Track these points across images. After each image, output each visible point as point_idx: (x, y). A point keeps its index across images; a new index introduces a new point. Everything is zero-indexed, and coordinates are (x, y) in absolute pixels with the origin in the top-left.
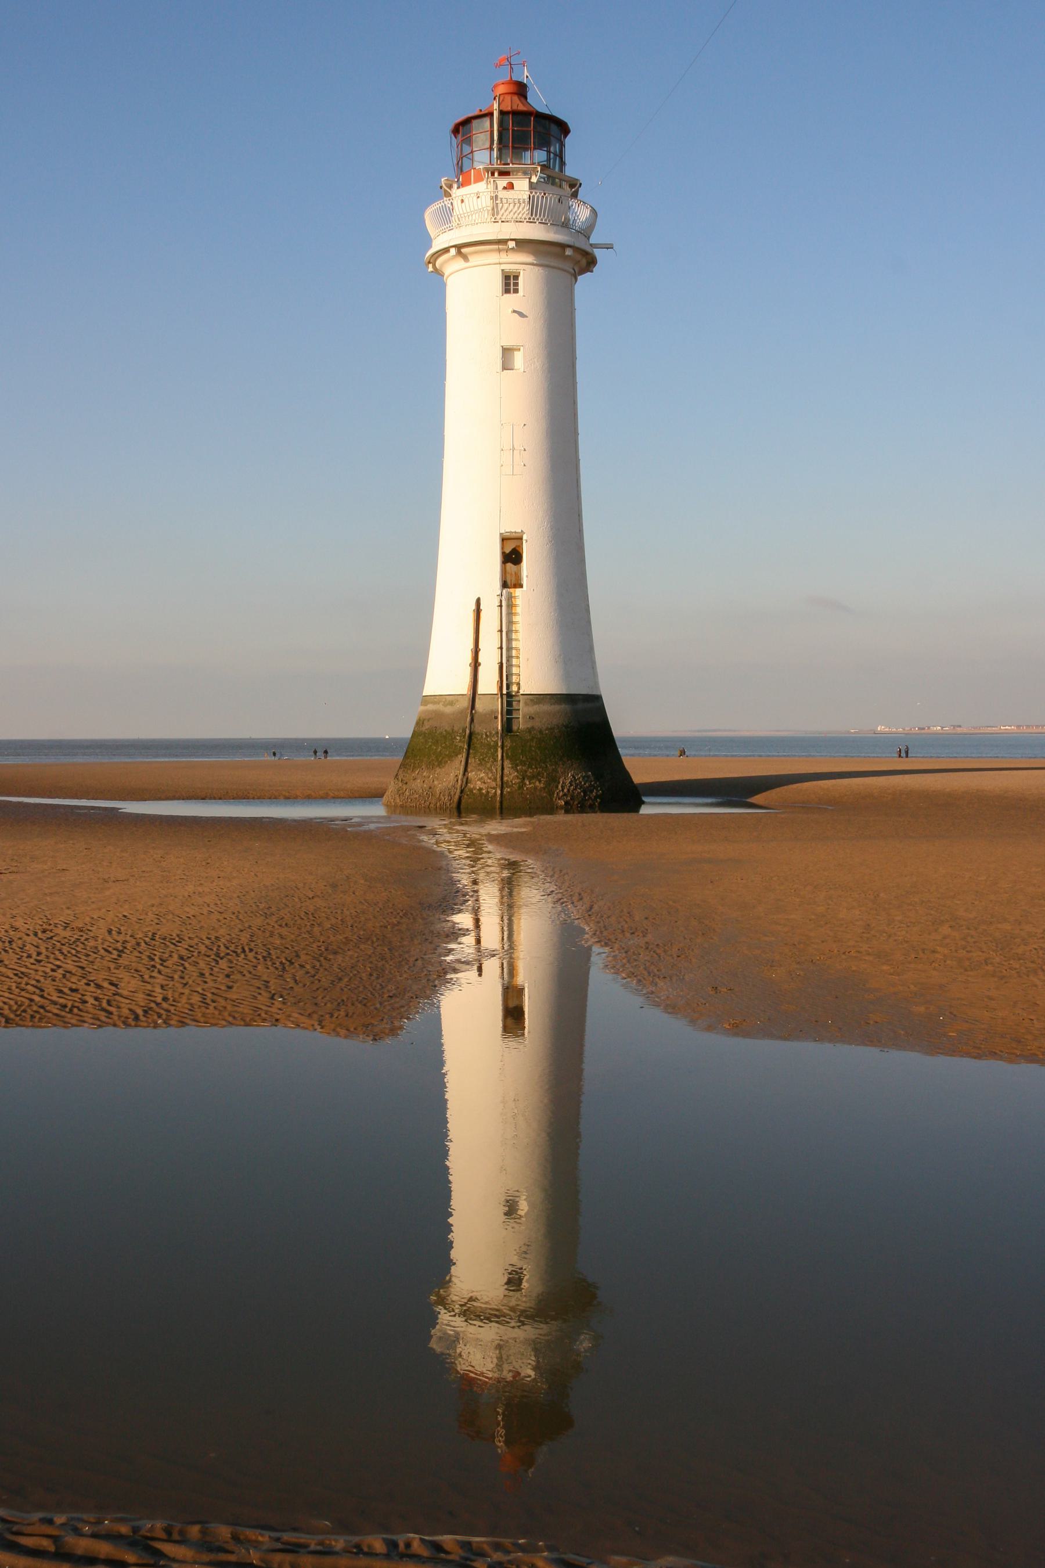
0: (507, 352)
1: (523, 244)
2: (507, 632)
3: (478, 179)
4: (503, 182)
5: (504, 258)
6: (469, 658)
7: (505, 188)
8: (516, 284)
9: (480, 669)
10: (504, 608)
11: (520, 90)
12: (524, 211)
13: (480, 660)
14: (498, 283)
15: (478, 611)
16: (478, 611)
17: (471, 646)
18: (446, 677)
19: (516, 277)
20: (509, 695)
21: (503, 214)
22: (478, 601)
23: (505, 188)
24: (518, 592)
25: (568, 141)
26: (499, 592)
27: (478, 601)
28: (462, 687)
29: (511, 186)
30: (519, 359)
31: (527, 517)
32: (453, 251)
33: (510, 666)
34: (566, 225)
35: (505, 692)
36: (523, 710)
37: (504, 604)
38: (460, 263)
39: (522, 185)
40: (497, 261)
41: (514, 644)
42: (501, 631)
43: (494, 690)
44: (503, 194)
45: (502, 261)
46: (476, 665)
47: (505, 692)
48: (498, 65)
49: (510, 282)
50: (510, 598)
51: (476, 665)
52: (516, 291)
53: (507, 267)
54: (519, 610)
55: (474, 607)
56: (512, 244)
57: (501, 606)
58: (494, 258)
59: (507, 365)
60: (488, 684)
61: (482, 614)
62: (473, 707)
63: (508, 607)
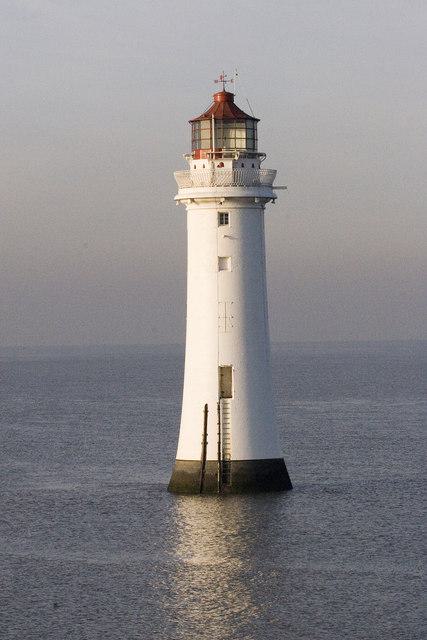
0: (221, 260)
1: (227, 199)
3: (203, 158)
4: (217, 163)
6: (202, 438)
8: (227, 219)
11: (228, 98)
12: (230, 179)
14: (215, 221)
15: (206, 412)
16: (206, 412)
18: (189, 449)
19: (227, 215)
20: (224, 461)
21: (218, 182)
24: (229, 400)
25: (259, 125)
28: (198, 457)
29: (222, 165)
30: (229, 263)
31: (231, 356)
32: (189, 201)
33: (225, 444)
34: (257, 184)
36: (232, 468)
39: (228, 164)
42: (219, 424)
46: (205, 443)
48: (216, 82)
49: (223, 219)
50: (225, 404)
51: (205, 443)
52: (227, 223)
55: (203, 409)
56: (222, 200)
58: (214, 205)
59: (220, 269)
60: (212, 456)
62: (204, 468)
63: (222, 410)
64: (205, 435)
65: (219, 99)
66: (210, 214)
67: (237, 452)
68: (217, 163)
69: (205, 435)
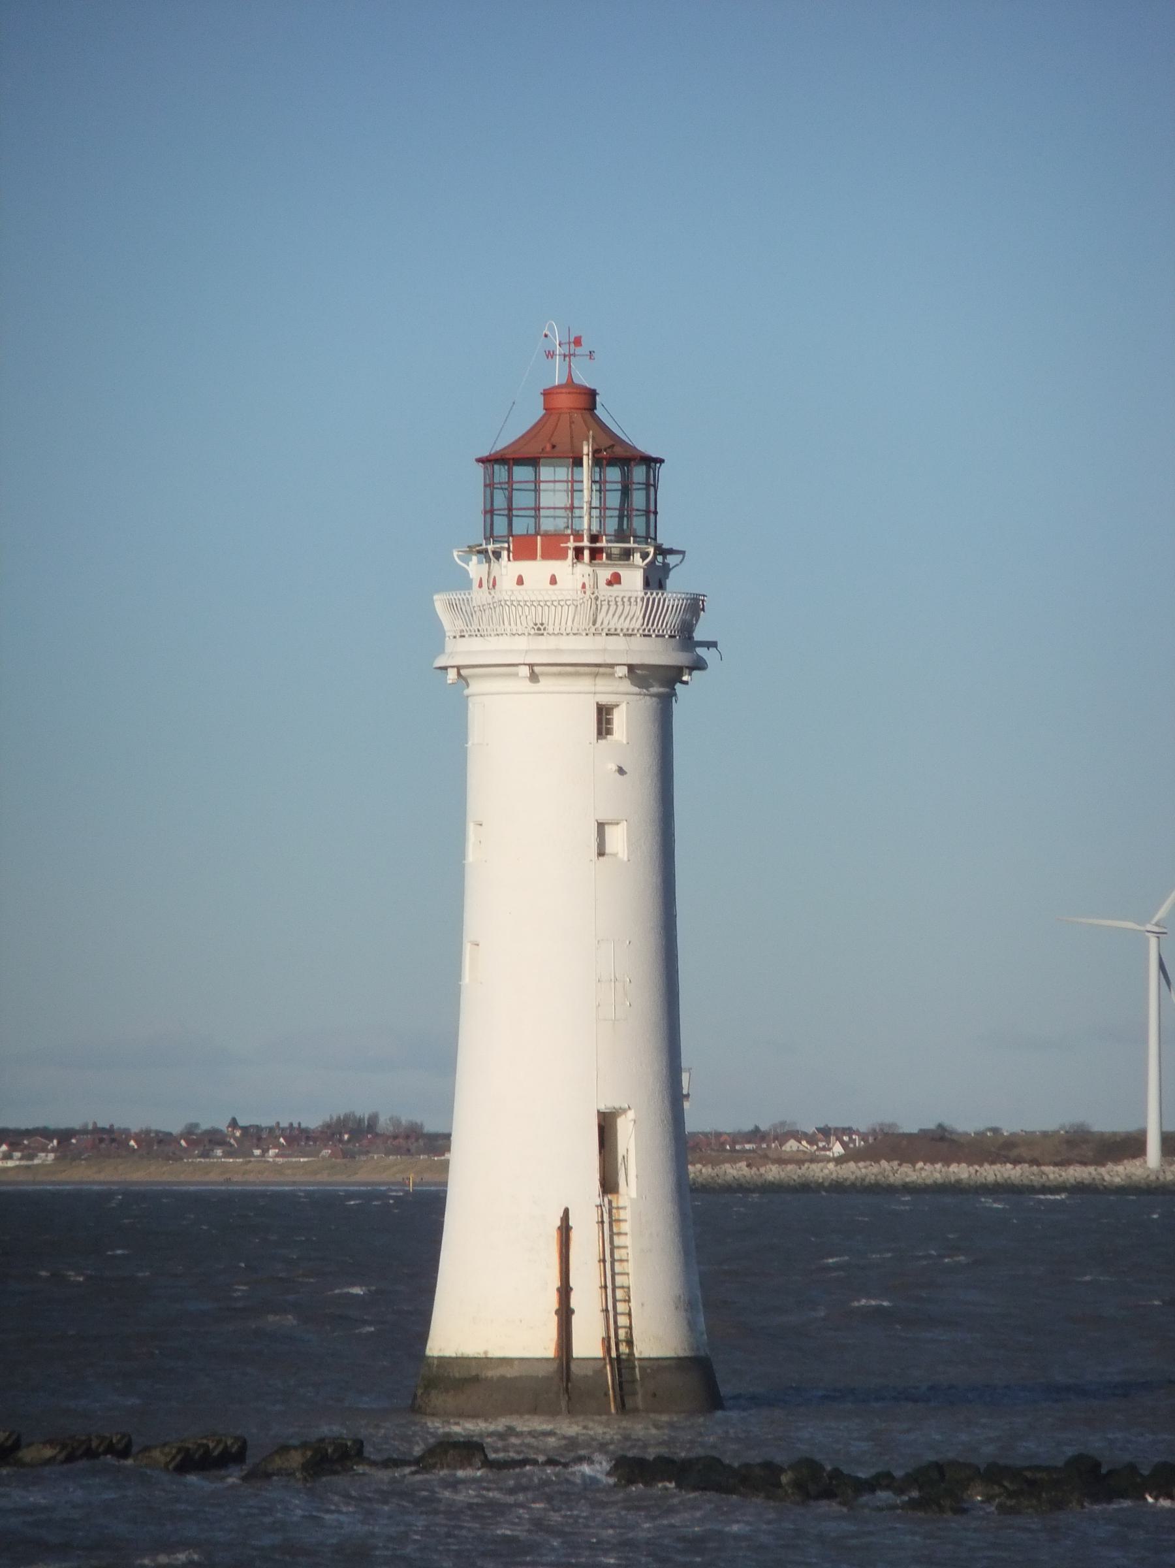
2: (609, 1259)
3: (554, 551)
4: (605, 574)
5: (603, 685)
6: (552, 1301)
7: (609, 583)
9: (575, 1319)
10: (606, 1226)
13: (573, 1305)
15: (565, 1231)
16: (565, 1231)
17: (555, 1282)
22: (566, 1211)
23: (610, 583)
26: (598, 1201)
27: (566, 1211)
28: (544, 1346)
29: (615, 580)
30: (617, 839)
35: (614, 1354)
37: (606, 1217)
38: (527, 685)
40: (592, 689)
41: (619, 1280)
43: (598, 1352)
44: (605, 591)
45: (599, 689)
46: (565, 1313)
47: (614, 1354)
51: (565, 1313)
52: (609, 732)
53: (605, 700)
54: (625, 1227)
57: (602, 1222)
58: (585, 684)
60: (588, 1343)
61: (574, 1235)
63: (609, 1222)
64: (565, 1291)
65: (564, 401)
66: (575, 703)
67: (656, 1335)
68: (605, 574)
69: (565, 1291)
